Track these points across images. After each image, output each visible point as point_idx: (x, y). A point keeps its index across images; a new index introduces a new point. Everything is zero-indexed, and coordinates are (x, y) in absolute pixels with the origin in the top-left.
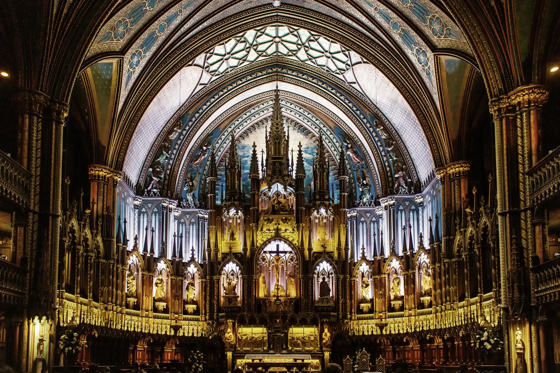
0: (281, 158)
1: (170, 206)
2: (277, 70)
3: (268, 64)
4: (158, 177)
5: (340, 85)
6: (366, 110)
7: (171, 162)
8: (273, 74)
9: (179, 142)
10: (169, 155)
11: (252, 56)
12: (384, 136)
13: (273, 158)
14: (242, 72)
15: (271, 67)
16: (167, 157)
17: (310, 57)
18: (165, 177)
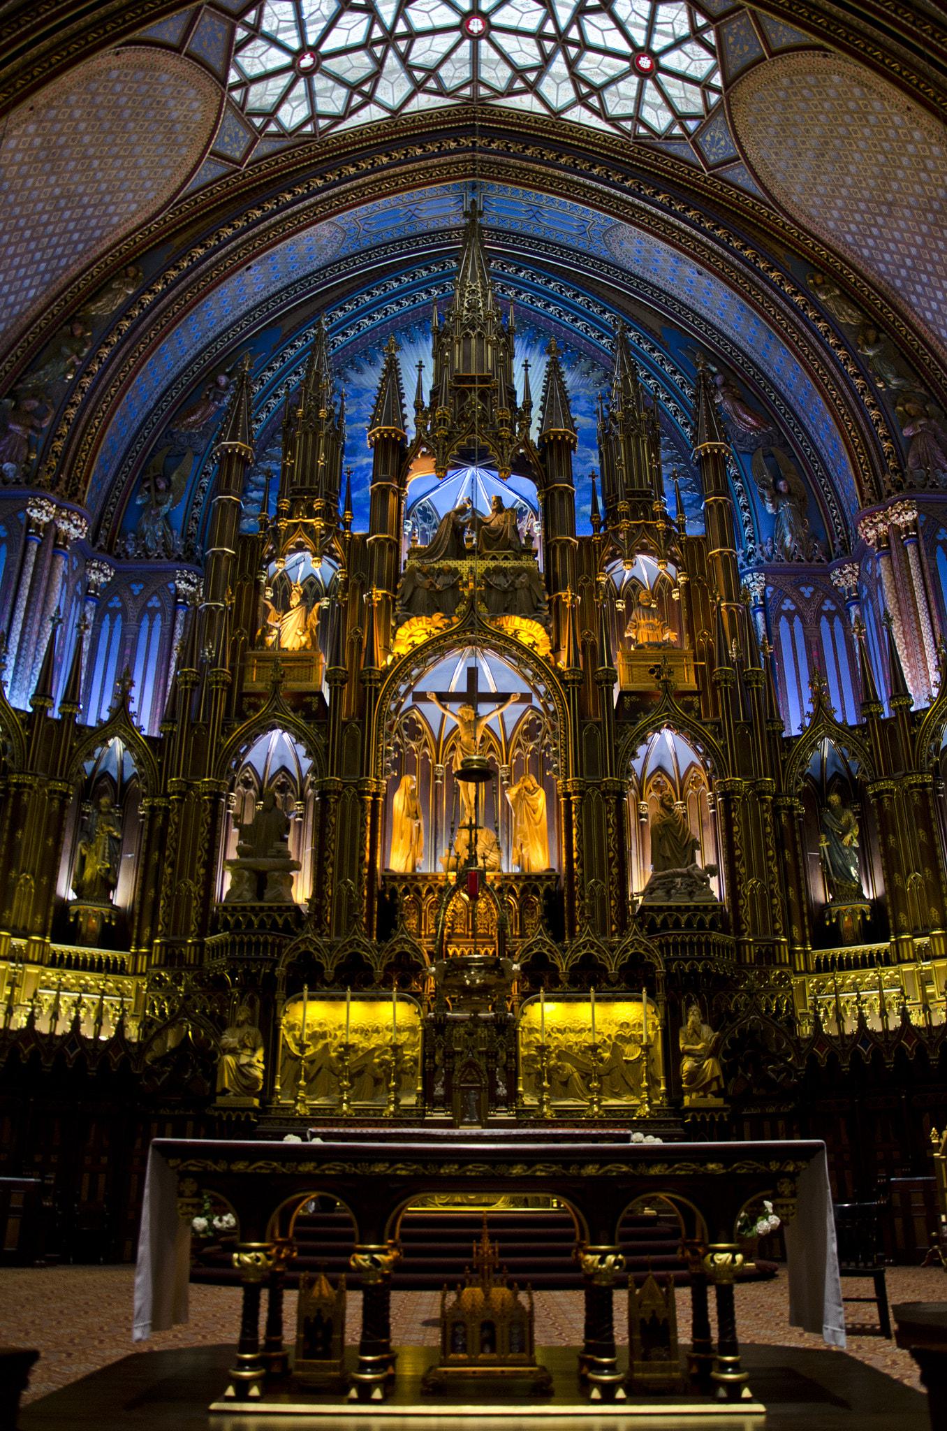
0: (484, 380)
1: (64, 526)
2: (474, 143)
3: (444, 123)
4: (32, 427)
5: (681, 178)
6: (777, 249)
7: (87, 382)
8: (461, 156)
9: (126, 324)
10: (80, 358)
11: (393, 90)
12: (848, 317)
13: (461, 380)
14: (360, 142)
15: (454, 134)
16: (73, 365)
17: (585, 90)
18: (55, 425)
